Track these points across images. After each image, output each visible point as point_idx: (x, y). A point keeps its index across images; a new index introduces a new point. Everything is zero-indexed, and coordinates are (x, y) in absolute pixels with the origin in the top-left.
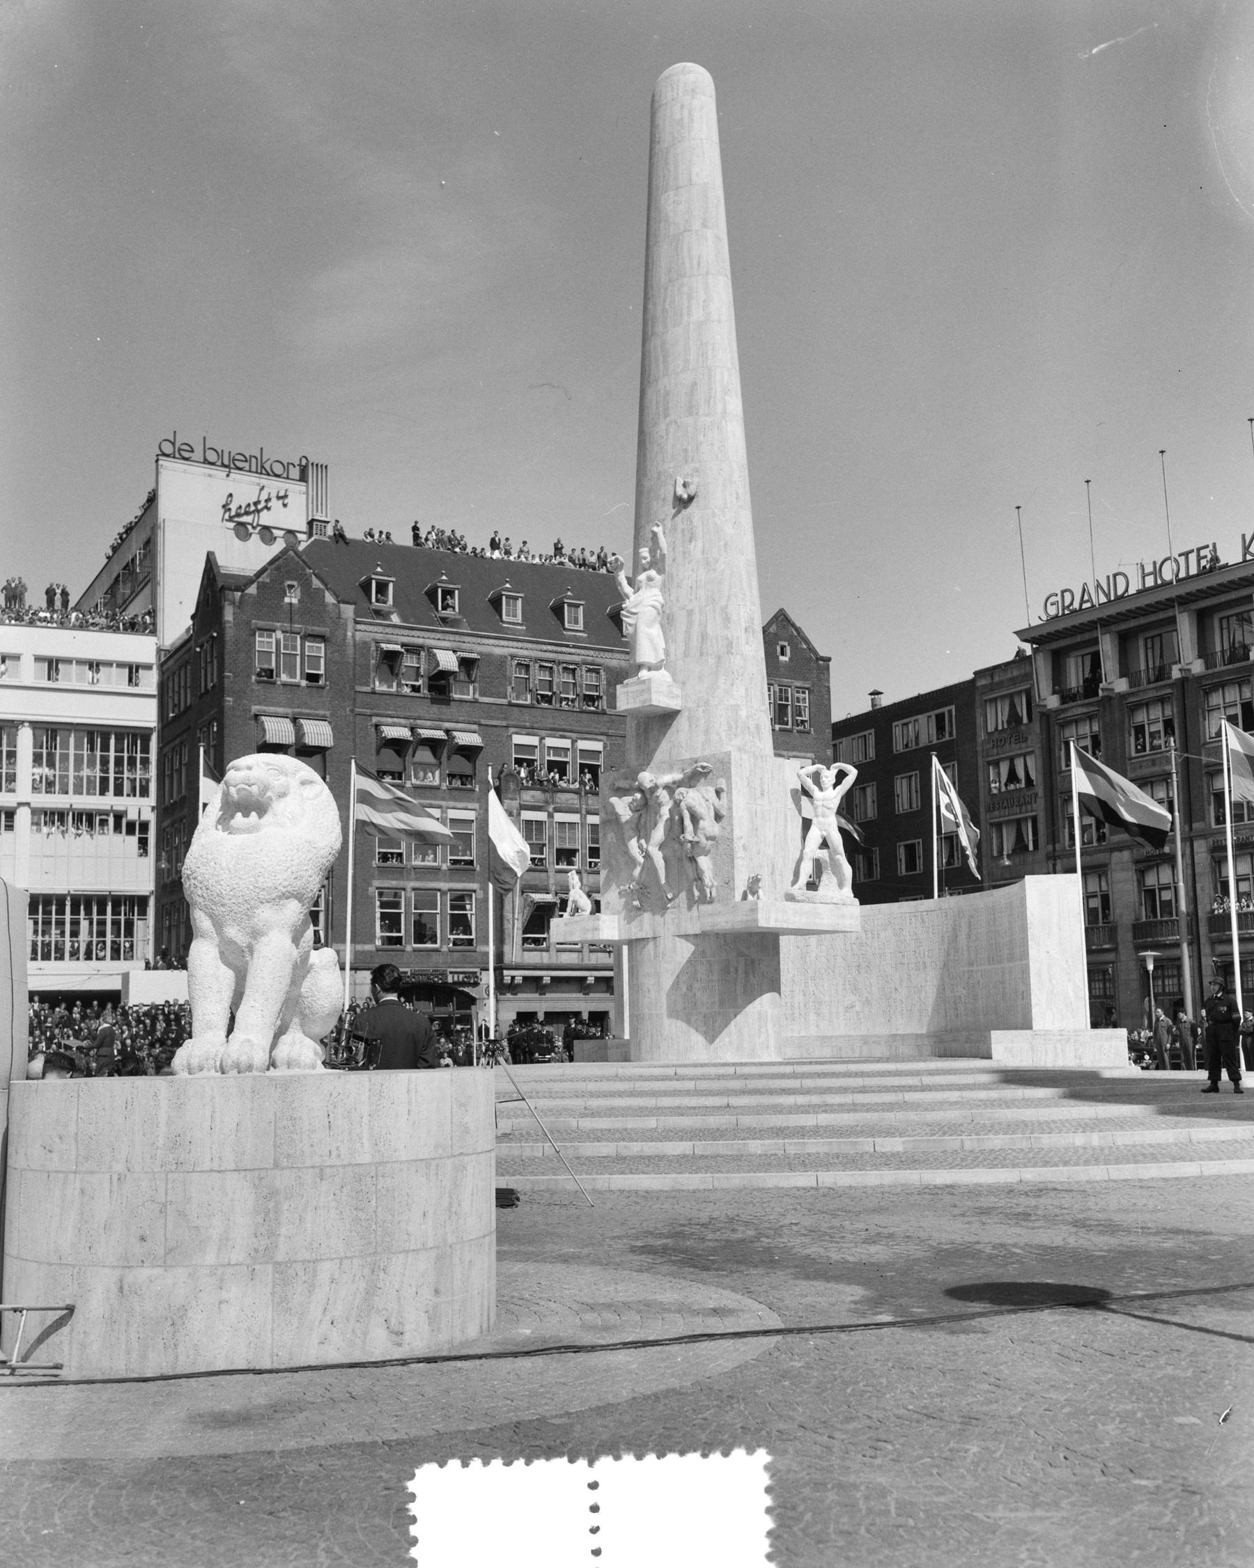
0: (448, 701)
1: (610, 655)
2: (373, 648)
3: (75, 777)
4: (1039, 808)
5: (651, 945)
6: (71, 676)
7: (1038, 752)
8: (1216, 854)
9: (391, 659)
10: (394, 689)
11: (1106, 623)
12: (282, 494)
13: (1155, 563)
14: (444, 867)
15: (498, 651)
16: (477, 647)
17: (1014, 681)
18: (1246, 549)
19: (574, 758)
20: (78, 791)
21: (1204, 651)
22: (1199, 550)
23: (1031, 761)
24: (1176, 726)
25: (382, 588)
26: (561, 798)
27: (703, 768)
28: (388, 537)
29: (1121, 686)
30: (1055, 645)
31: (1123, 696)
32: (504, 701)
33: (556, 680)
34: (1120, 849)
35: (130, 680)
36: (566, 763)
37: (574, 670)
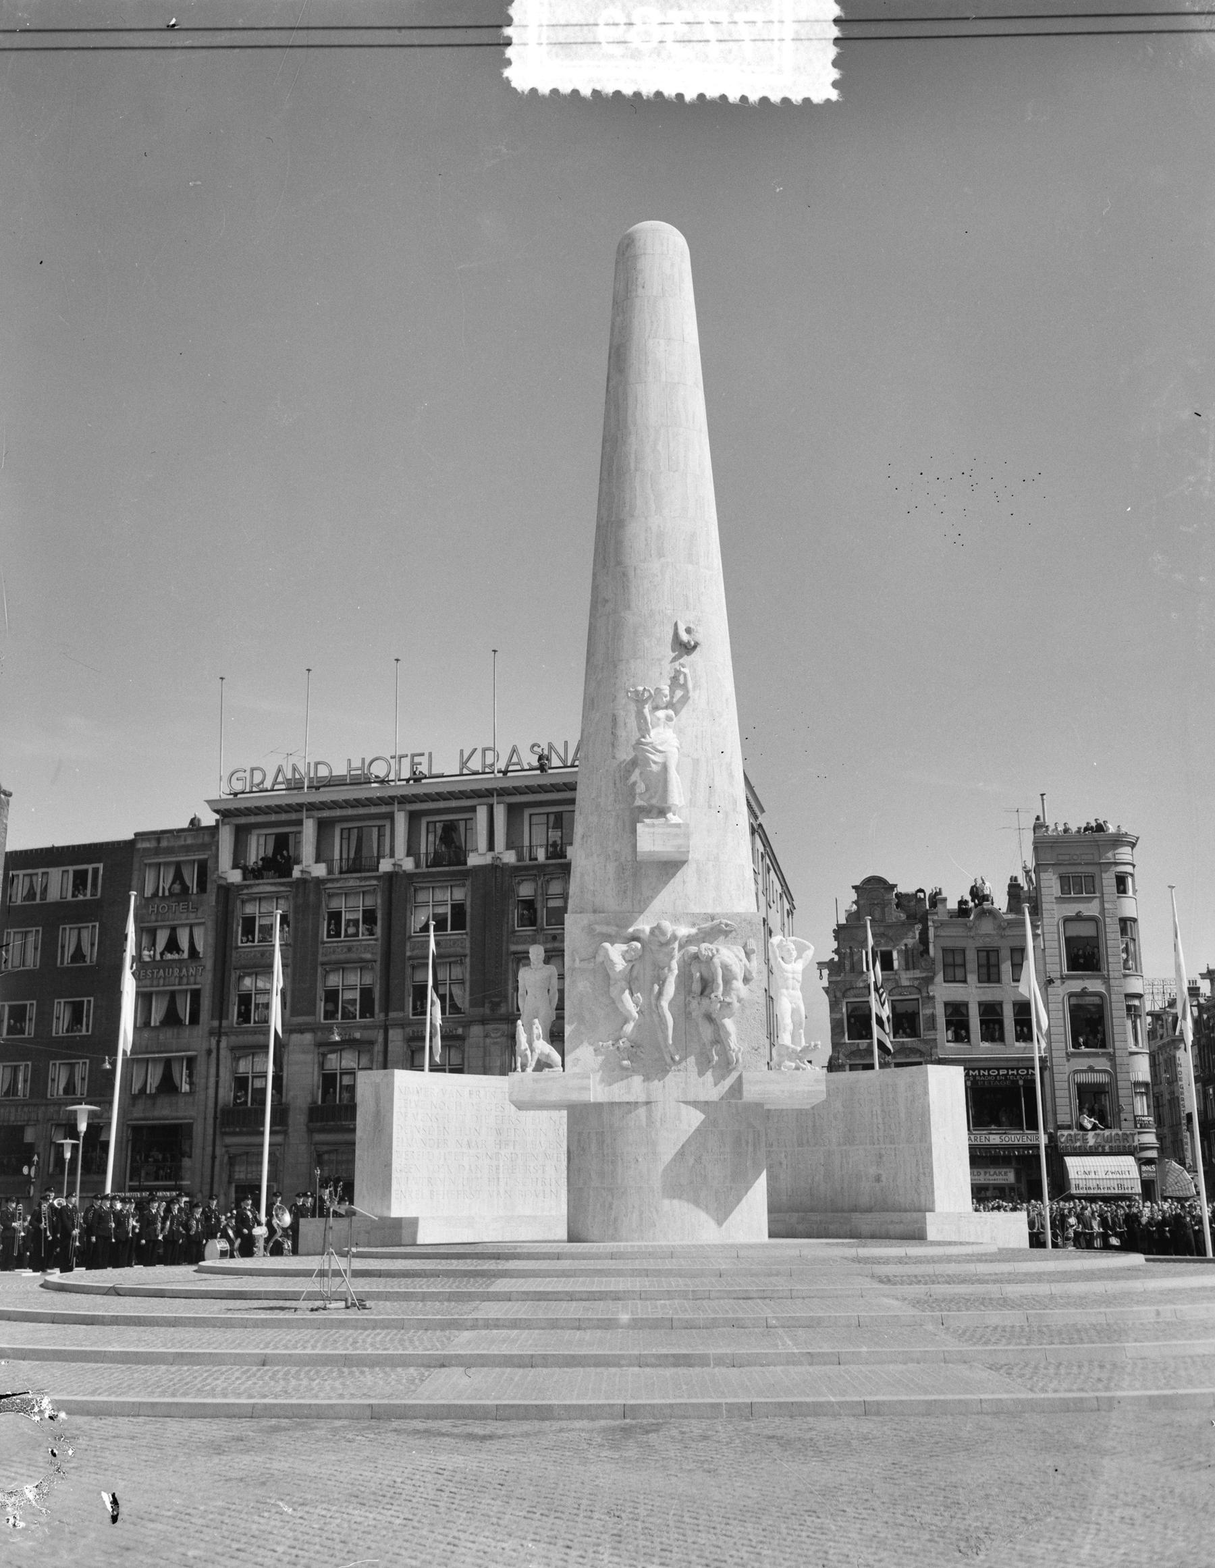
4: (205, 980)
5: (642, 1111)
7: (210, 924)
8: (412, 1044)
11: (312, 807)
13: (363, 760)
17: (187, 849)
18: (464, 764)
21: (411, 851)
22: (413, 756)
23: (199, 933)
24: (379, 916)
27: (727, 925)
29: (320, 871)
30: (243, 820)
31: (319, 881)
34: (302, 1032)
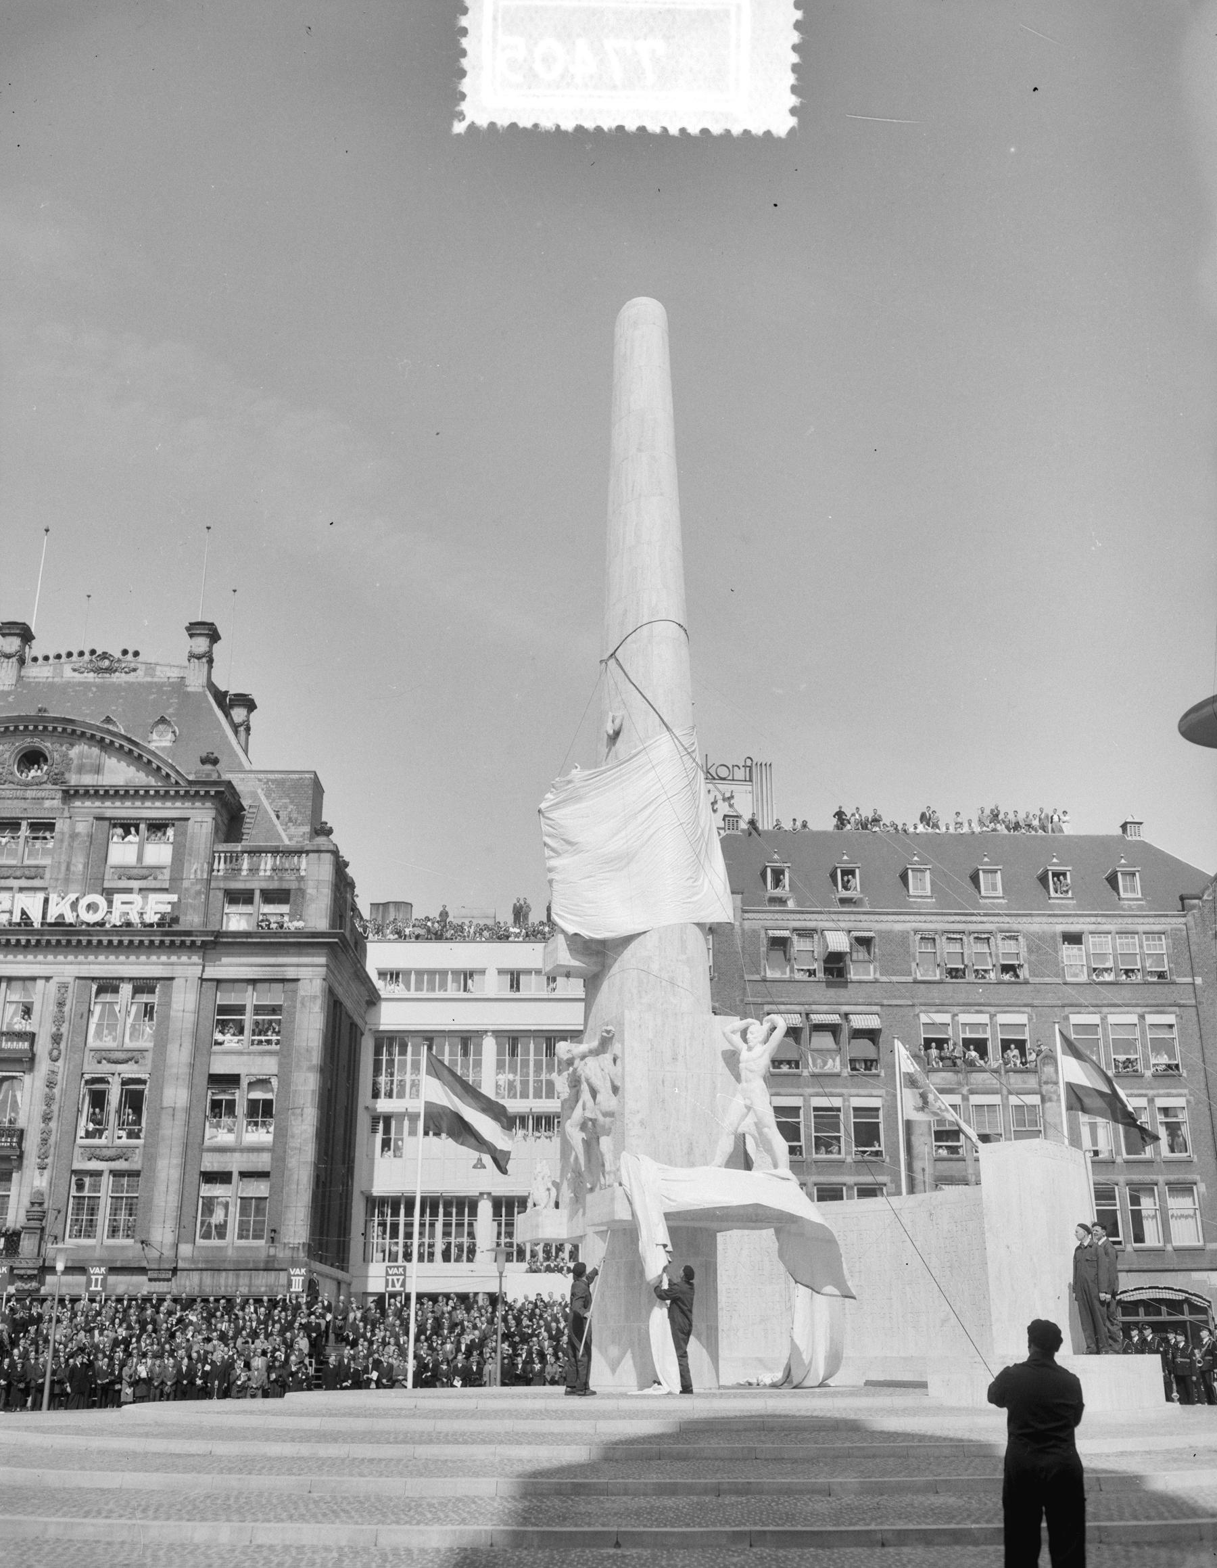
0: (845, 984)
1: (1029, 919)
2: (763, 935)
3: (535, 1081)
6: (532, 986)
9: (780, 944)
10: (787, 976)
12: (727, 795)
14: (849, 1159)
15: (898, 927)
16: (869, 925)
19: (994, 1034)
20: (538, 1095)
25: (778, 874)
26: (978, 1078)
28: (804, 825)
32: (910, 979)
33: (966, 952)
35: (512, 986)
36: (986, 1039)
37: (988, 939)
